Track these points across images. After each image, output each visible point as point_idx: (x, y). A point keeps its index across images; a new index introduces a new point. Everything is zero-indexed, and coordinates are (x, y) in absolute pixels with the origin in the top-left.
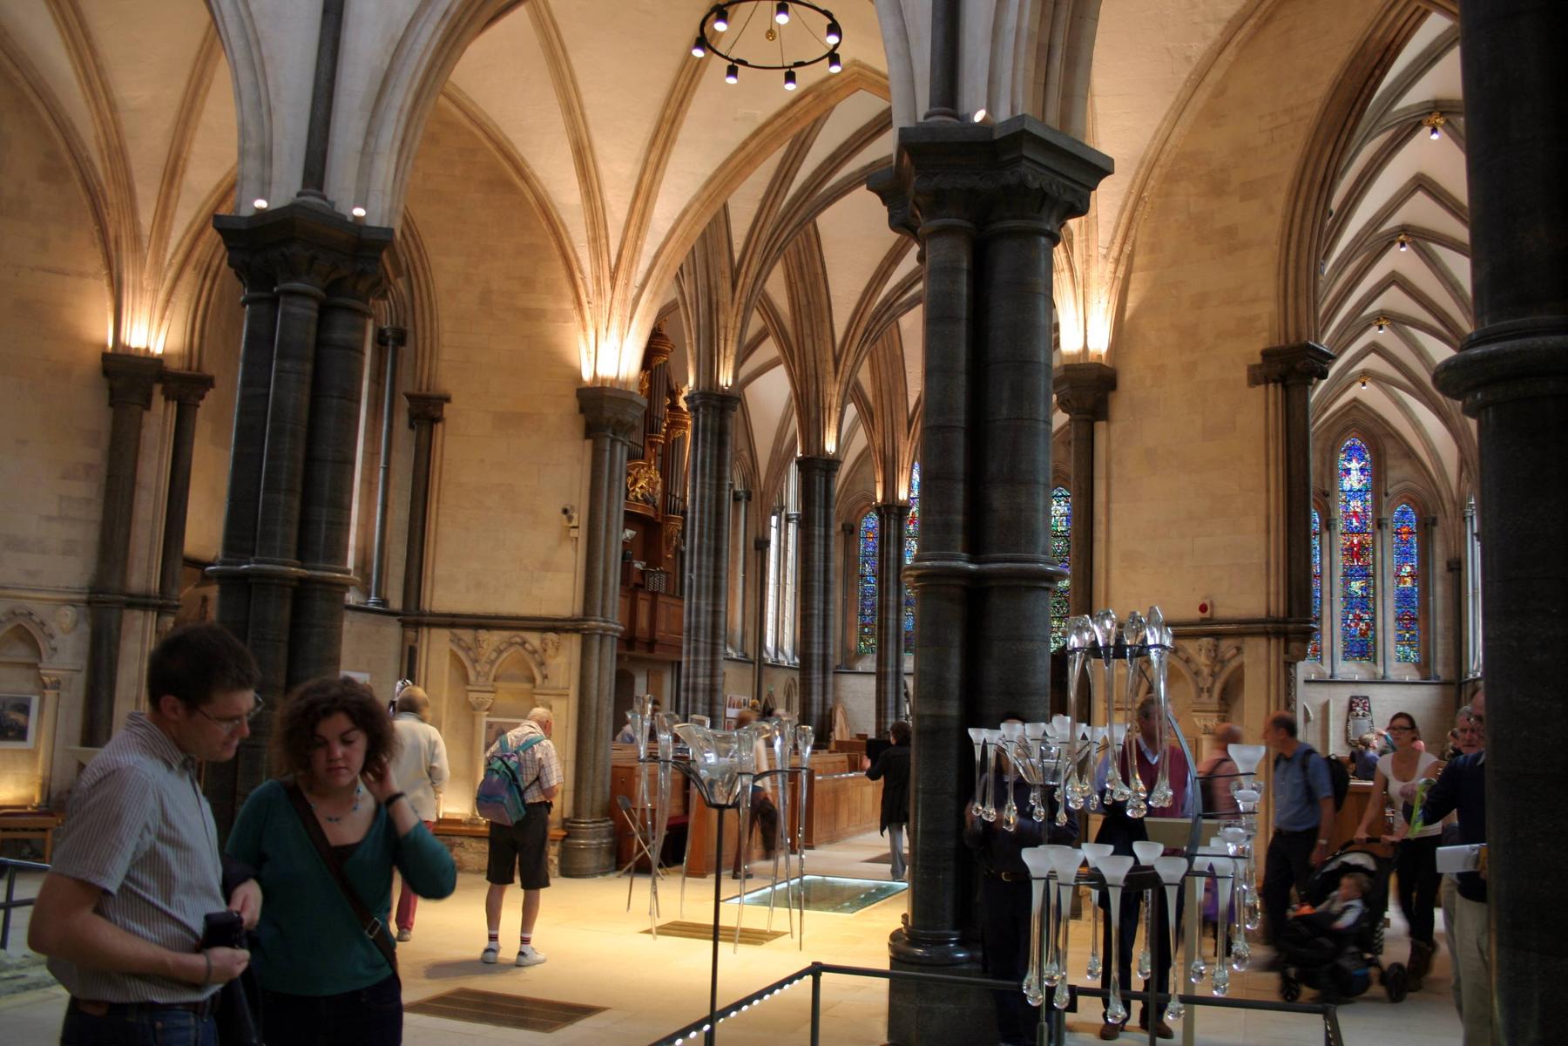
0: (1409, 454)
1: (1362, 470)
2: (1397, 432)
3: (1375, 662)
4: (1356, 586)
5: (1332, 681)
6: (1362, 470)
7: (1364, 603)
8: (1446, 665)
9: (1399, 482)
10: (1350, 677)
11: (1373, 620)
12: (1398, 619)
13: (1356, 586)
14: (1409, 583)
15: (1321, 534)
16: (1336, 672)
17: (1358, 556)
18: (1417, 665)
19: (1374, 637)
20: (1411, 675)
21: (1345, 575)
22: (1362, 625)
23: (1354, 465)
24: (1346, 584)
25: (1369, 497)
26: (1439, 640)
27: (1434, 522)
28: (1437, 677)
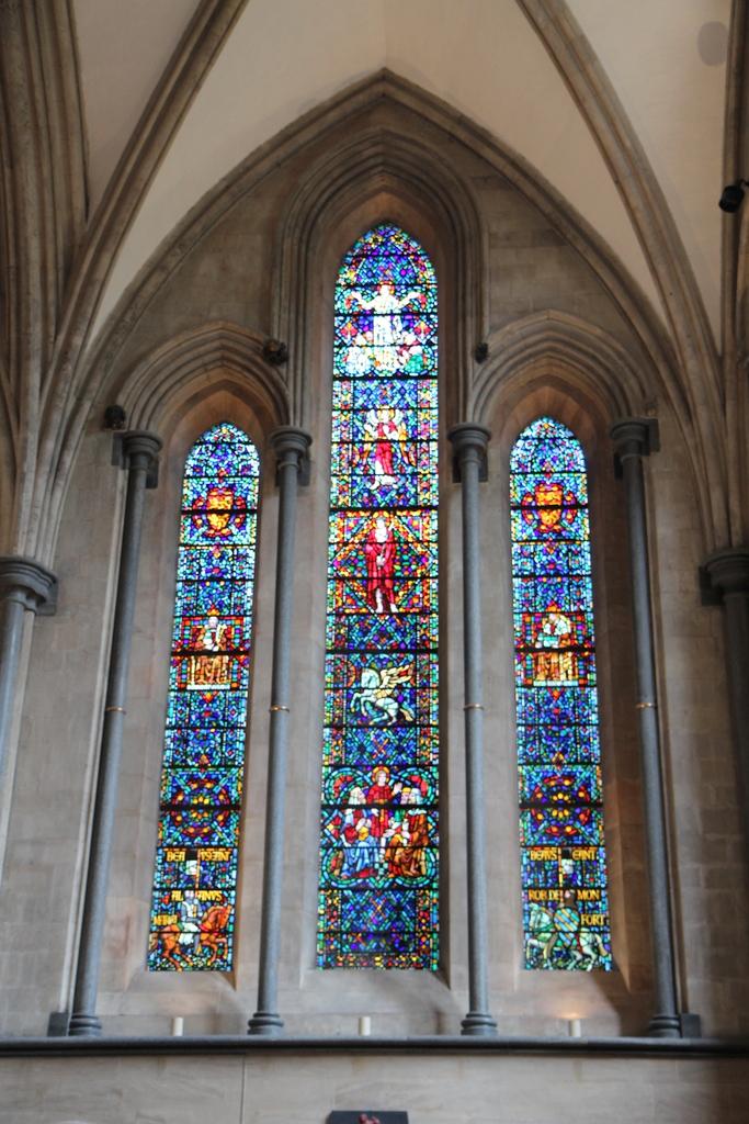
0: (559, 227)
1: (409, 316)
2: (517, 164)
3: (443, 974)
4: (378, 687)
5: (256, 1046)
6: (409, 316)
7: (403, 758)
8: (719, 967)
9: (523, 314)
10: (345, 1031)
11: (438, 807)
12: (531, 805)
13: (378, 687)
14: (565, 671)
15: (258, 512)
16: (279, 1006)
17: (387, 582)
18: (607, 980)
19: (443, 867)
20: (577, 1011)
21: (342, 647)
22: (399, 830)
23: (385, 301)
24: (345, 685)
25: (431, 393)
26: (689, 867)
27: (648, 439)
28: (686, 1021)
